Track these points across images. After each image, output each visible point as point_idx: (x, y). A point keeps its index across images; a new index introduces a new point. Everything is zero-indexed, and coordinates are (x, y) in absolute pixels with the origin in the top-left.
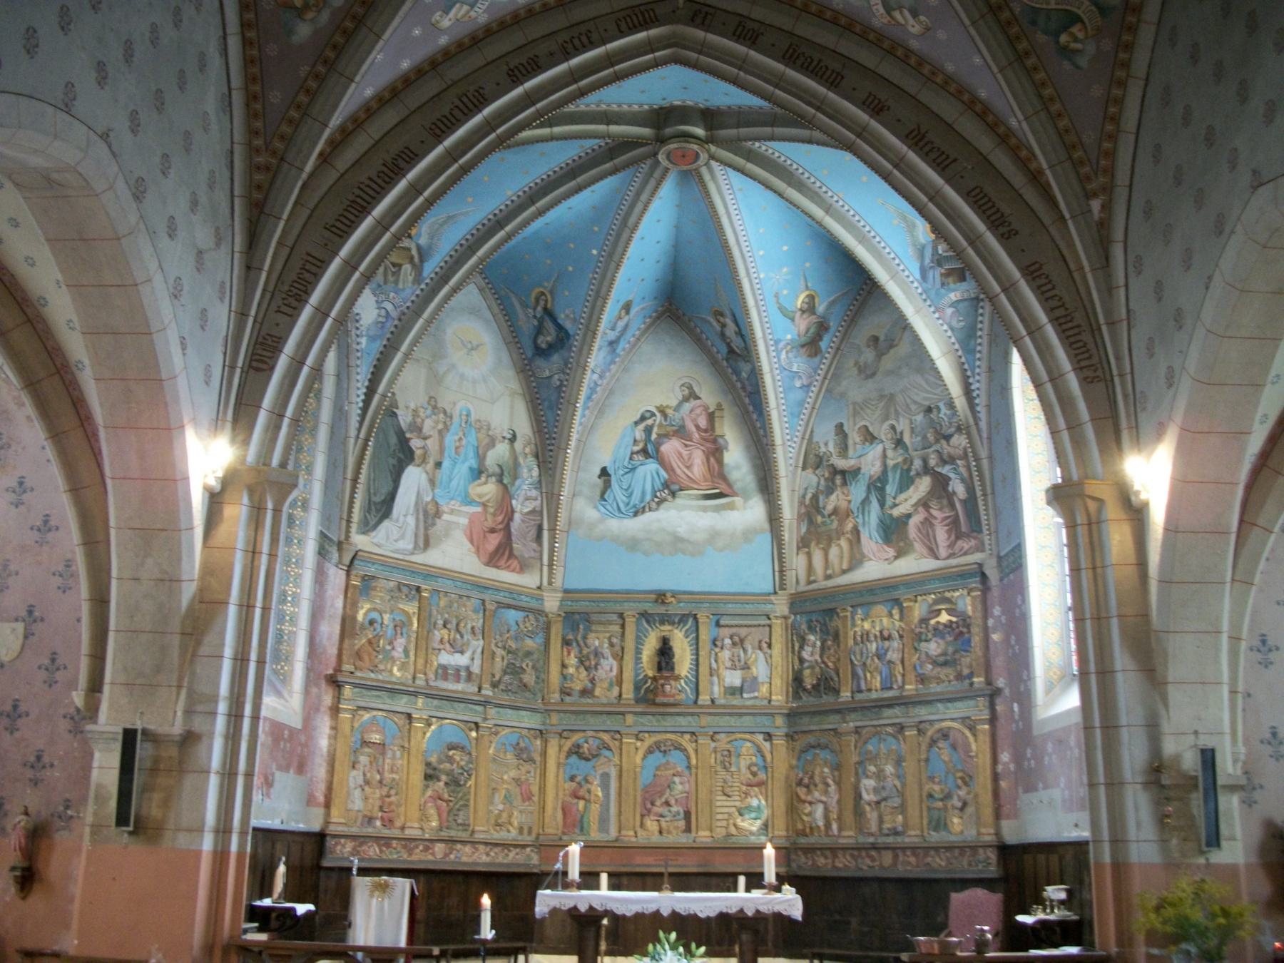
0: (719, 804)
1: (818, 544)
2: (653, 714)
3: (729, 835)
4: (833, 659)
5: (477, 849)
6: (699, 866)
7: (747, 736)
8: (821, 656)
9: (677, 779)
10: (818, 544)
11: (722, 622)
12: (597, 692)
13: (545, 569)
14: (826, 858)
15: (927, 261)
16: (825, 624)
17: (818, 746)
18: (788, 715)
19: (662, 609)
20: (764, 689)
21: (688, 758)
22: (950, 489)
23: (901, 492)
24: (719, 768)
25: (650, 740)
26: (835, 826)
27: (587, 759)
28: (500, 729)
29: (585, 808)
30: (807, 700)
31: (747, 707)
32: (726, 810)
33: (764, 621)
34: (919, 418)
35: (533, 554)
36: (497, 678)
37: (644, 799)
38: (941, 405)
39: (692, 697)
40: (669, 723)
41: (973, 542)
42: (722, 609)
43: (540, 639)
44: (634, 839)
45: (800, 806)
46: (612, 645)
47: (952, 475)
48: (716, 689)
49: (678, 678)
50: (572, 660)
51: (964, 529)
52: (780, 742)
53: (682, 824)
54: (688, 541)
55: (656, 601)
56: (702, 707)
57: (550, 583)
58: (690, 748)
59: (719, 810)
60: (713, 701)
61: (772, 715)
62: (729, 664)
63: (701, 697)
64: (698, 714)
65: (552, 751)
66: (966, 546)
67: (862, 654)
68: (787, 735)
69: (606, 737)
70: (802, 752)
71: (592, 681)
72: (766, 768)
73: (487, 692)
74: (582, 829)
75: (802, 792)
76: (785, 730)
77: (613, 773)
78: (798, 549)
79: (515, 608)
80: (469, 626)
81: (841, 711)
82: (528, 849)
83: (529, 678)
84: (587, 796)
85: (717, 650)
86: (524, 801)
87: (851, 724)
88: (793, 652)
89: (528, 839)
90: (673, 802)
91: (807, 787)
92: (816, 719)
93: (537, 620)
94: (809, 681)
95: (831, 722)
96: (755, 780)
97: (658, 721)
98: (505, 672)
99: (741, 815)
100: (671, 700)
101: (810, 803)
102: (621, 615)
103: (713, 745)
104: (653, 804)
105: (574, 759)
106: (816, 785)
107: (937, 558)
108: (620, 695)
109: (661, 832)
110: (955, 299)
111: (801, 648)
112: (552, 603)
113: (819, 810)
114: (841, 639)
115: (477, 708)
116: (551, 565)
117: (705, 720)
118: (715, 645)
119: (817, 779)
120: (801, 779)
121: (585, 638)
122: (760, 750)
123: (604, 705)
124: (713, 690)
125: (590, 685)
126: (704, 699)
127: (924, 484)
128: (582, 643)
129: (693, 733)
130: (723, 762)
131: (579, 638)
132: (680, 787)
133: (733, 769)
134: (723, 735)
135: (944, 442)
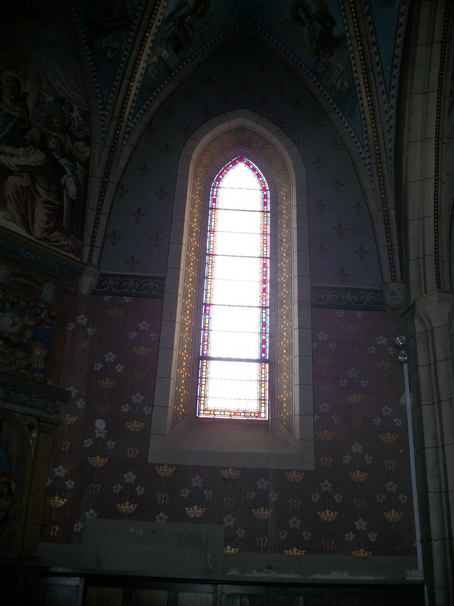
15: (178, 14)
22: (63, 180)
23: (8, 144)
34: (50, 99)
38: (75, 107)
41: (70, 242)
47: (68, 170)
51: (64, 224)
66: (62, 243)
107: (31, 235)
110: (163, 56)
127: (36, 158)
135: (69, 141)
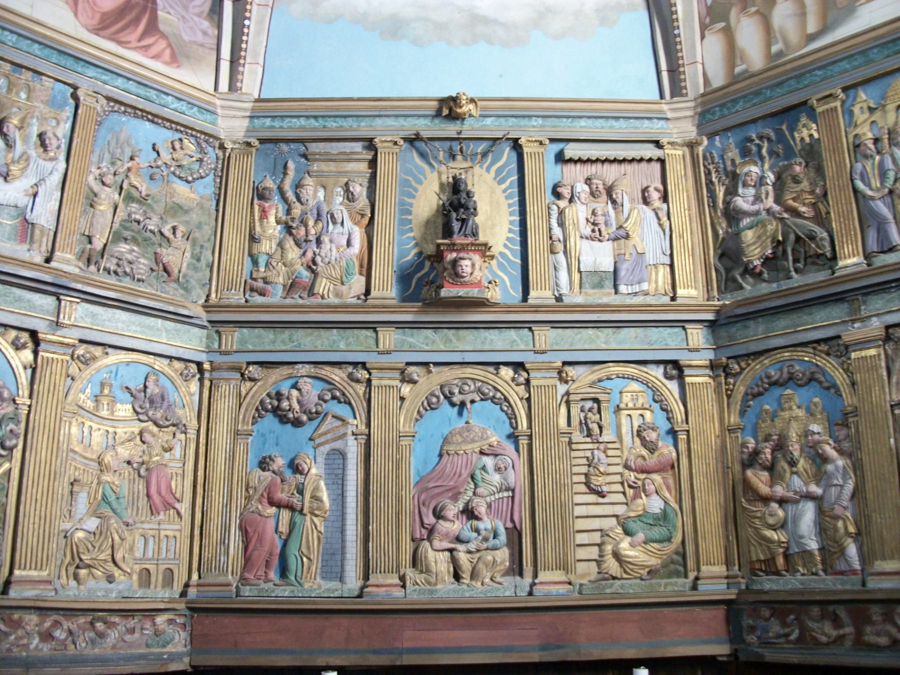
0: (579, 511)
1: (744, 8)
2: (436, 326)
3: (605, 577)
4: (810, 199)
5: (18, 624)
6: (544, 648)
7: (631, 370)
8: (777, 201)
9: (489, 461)
10: (744, 8)
11: (568, 154)
12: (323, 286)
13: (225, 66)
14: (837, 622)
16: (781, 138)
17: (791, 380)
18: (712, 325)
19: (450, 129)
20: (662, 276)
21: (512, 417)
24: (577, 436)
25: (429, 382)
26: (852, 550)
27: (297, 423)
28: (98, 351)
29: (292, 525)
30: (749, 288)
31: (630, 309)
32: (596, 524)
33: (650, 151)
35: (200, 38)
36: (98, 244)
37: (421, 504)
39: (516, 295)
40: (469, 343)
42: (565, 128)
43: (207, 187)
44: (398, 593)
45: (758, 508)
46: (350, 197)
48: (563, 276)
49: (484, 249)
50: (272, 229)
52: (698, 379)
53: (503, 555)
54: (495, 22)
55: (438, 114)
56: (537, 309)
57: (232, 87)
58: (516, 395)
59: (580, 524)
60: (559, 299)
61: (682, 324)
62: (587, 230)
63: (533, 294)
64: (528, 325)
65: (224, 406)
67: (883, 175)
68: (713, 366)
69: (337, 376)
70: (754, 395)
71: (311, 268)
72: (673, 433)
73: (67, 262)
74: (284, 571)
75: (759, 479)
76: (707, 356)
77: (353, 449)
78: (703, 28)
79: (154, 118)
80: (35, 130)
81: (850, 295)
82: (161, 619)
83: (177, 256)
84: (296, 501)
85: (563, 204)
86: (153, 510)
87: (875, 323)
88: (713, 205)
89: (160, 594)
90: (482, 510)
91: (771, 468)
92: (783, 323)
93: (202, 151)
94: (755, 250)
95: (822, 322)
96: (652, 460)
97: (448, 341)
98: (117, 237)
99: (628, 533)
100: (474, 292)
101: (782, 502)
102: (370, 144)
103: (562, 389)
104: (439, 514)
105: (270, 421)
106: (793, 463)
108: (368, 292)
109: (457, 577)
111: (731, 192)
112: (232, 126)
113: (808, 513)
114: (826, 155)
115: (37, 298)
116: (234, 61)
117: (546, 337)
118: (557, 195)
119: (795, 449)
120: (756, 453)
121: (298, 186)
122: (658, 399)
123: (334, 308)
124: (555, 281)
125: (306, 274)
126: (539, 294)
128: (291, 195)
129: (518, 366)
130: (584, 424)
131: (287, 186)
132: (496, 478)
133: (608, 436)
134: (581, 369)
